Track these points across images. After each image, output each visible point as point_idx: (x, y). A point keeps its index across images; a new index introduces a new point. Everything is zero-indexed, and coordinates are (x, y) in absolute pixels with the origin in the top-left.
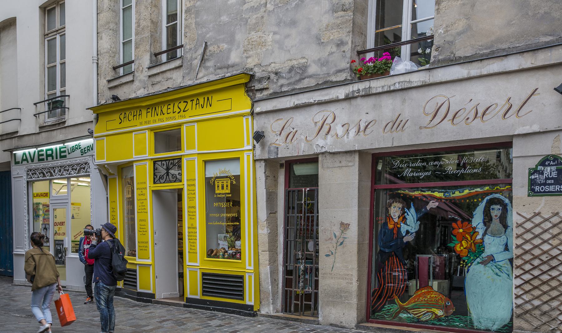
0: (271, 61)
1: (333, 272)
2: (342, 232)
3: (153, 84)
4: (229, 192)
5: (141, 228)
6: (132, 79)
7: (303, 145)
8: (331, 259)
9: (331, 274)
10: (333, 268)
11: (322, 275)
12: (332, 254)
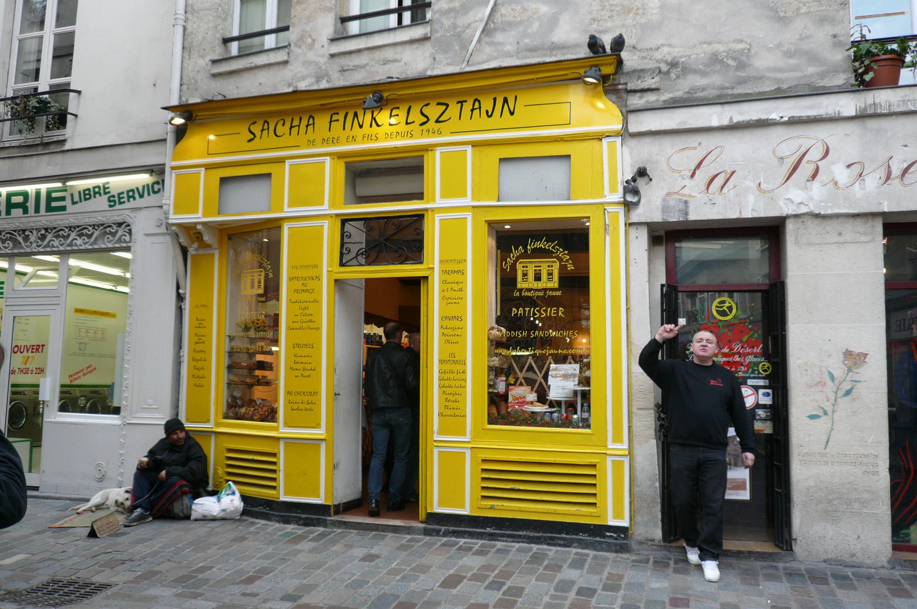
0: (661, 41)
1: (828, 450)
2: (850, 370)
3: (344, 71)
4: (556, 285)
5: (295, 362)
6: (285, 58)
7: (751, 198)
8: (822, 425)
9: (824, 455)
10: (827, 442)
11: (801, 458)
12: (826, 413)
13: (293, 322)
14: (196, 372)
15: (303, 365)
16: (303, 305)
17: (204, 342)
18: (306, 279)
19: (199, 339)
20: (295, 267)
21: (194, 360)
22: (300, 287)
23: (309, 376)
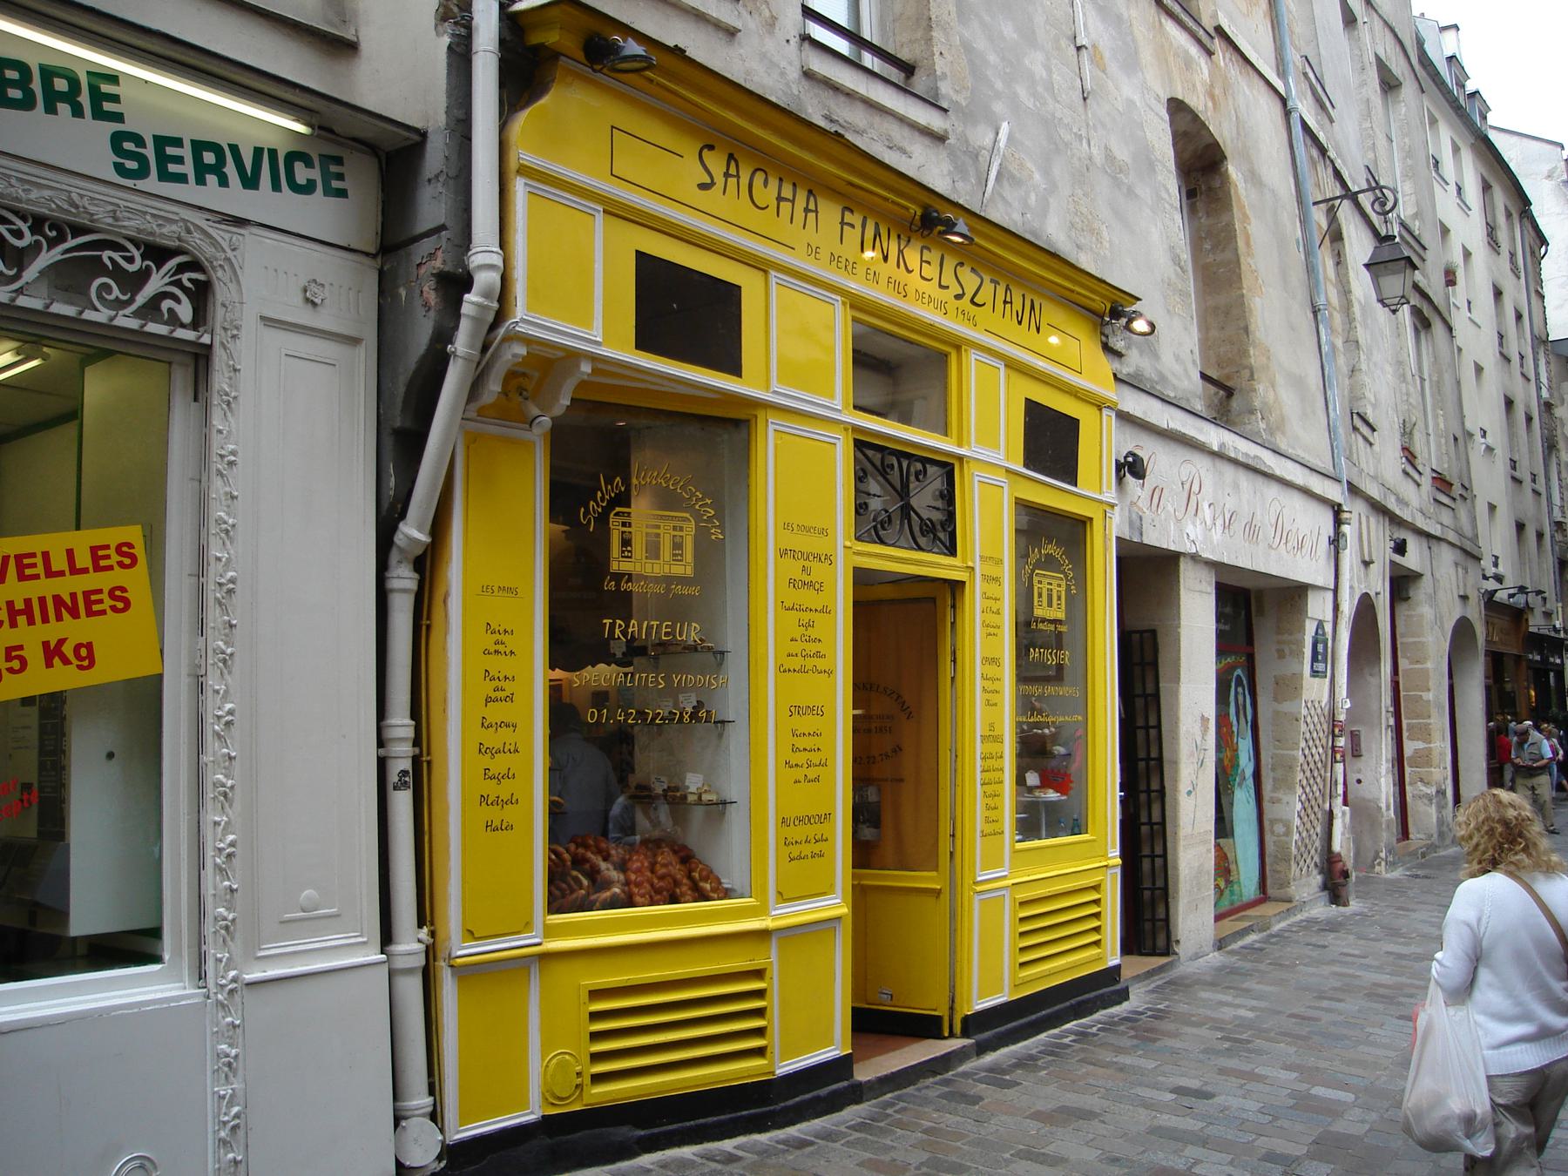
5: (795, 749)
13: (789, 655)
14: (491, 789)
20: (787, 526)
21: (482, 750)
22: (798, 575)
23: (817, 779)
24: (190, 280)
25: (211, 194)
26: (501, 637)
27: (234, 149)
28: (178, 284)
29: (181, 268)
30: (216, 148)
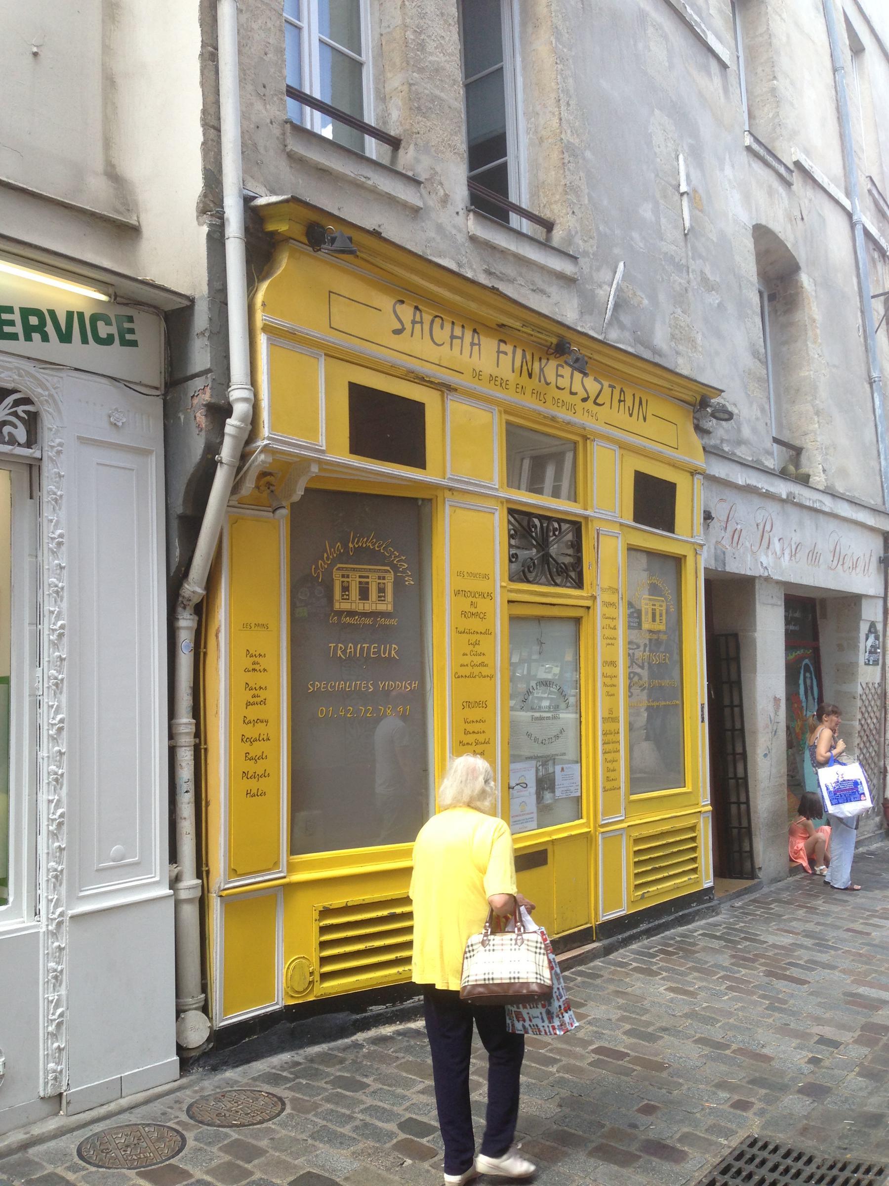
5: (466, 732)
13: (462, 666)
14: (250, 767)
15: (475, 736)
16: (474, 638)
17: (264, 702)
18: (475, 596)
19: (253, 696)
20: (460, 574)
21: (244, 740)
22: (468, 609)
24: (24, 411)
25: (36, 347)
26: (256, 659)
27: (52, 313)
28: (15, 414)
29: (17, 403)
30: (37, 313)
